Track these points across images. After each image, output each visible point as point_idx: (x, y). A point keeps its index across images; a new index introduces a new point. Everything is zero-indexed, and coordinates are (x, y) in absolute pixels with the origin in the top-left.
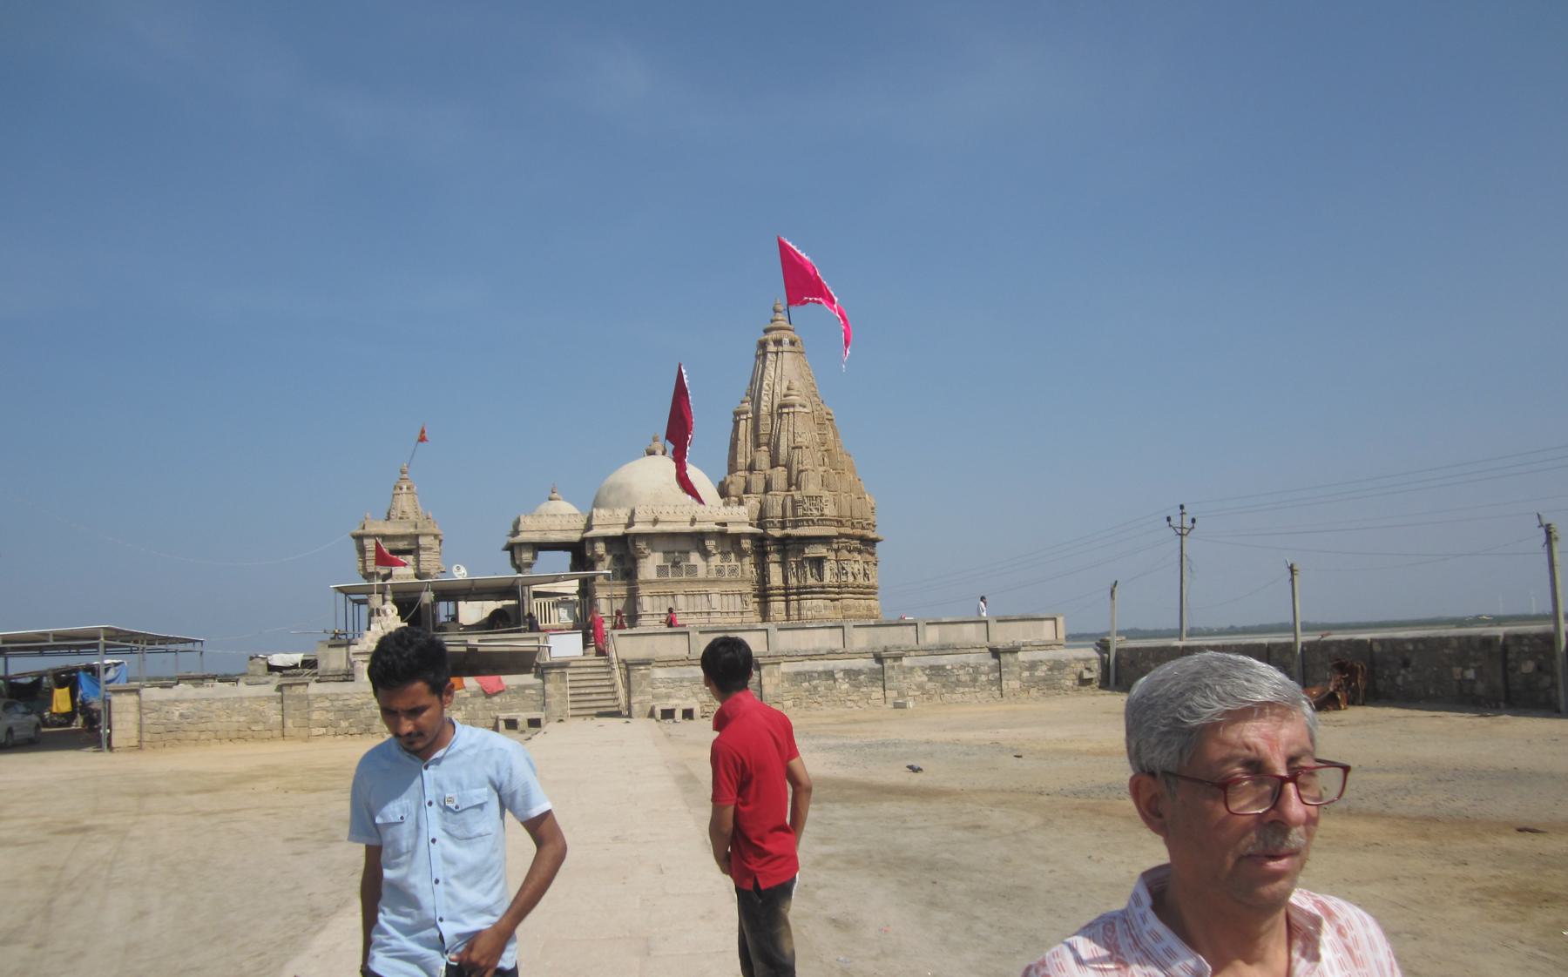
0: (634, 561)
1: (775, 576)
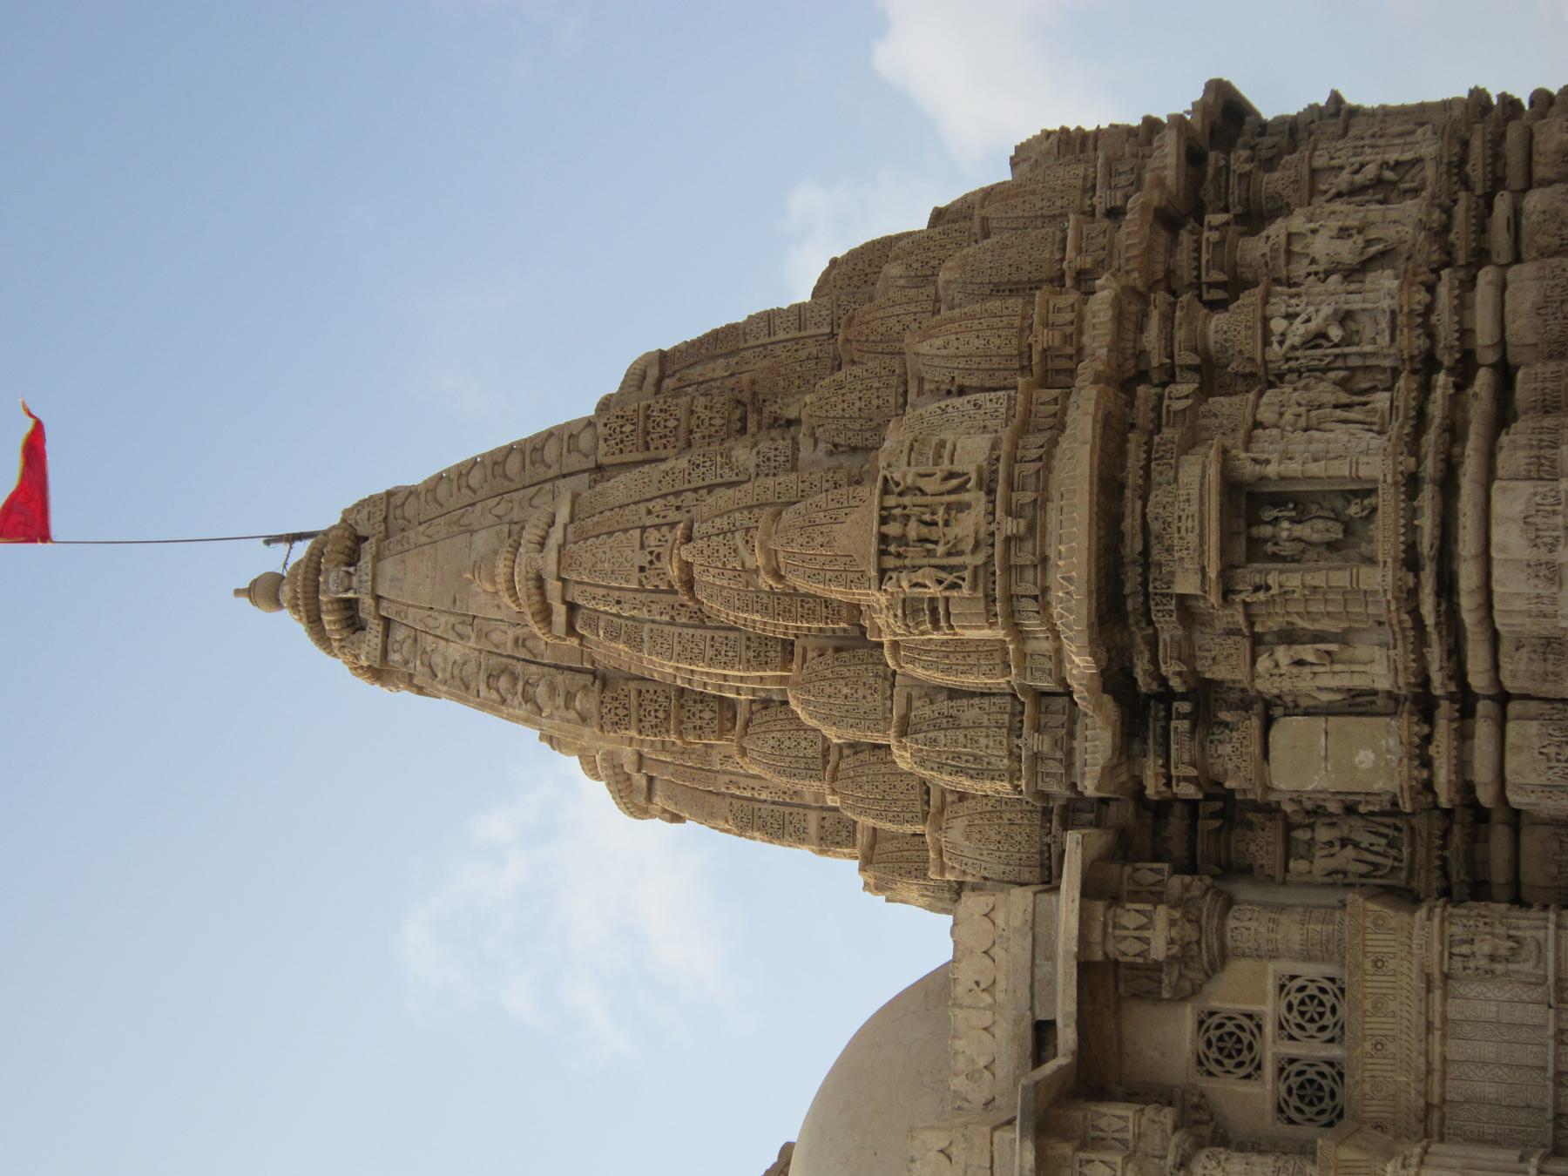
1: (1333, 760)
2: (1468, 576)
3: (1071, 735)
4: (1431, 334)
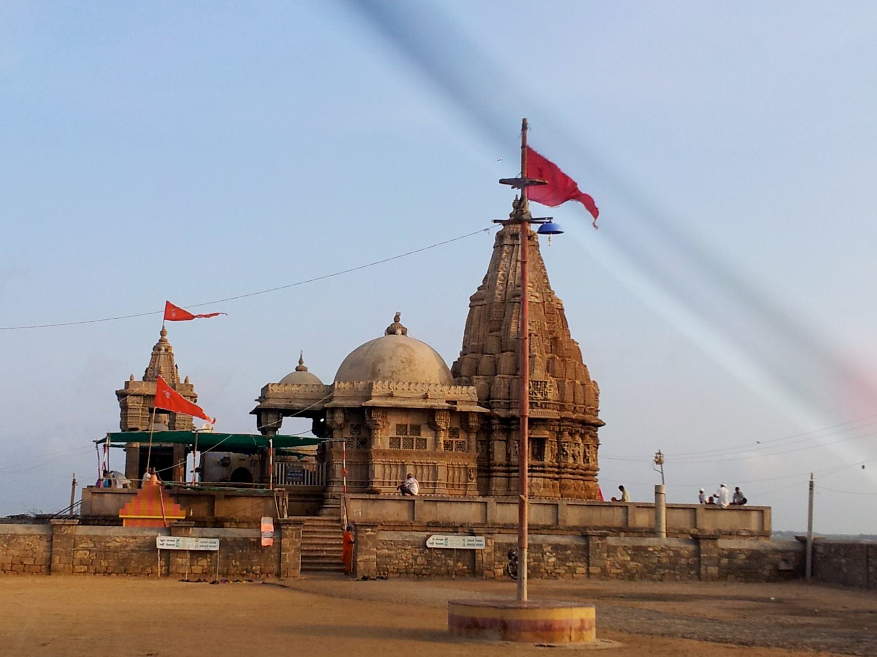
0: (370, 431)
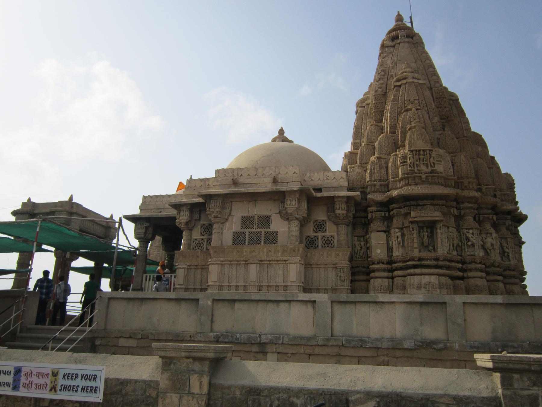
1: (377, 245)
2: (417, 271)
3: (380, 192)
4: (470, 263)
